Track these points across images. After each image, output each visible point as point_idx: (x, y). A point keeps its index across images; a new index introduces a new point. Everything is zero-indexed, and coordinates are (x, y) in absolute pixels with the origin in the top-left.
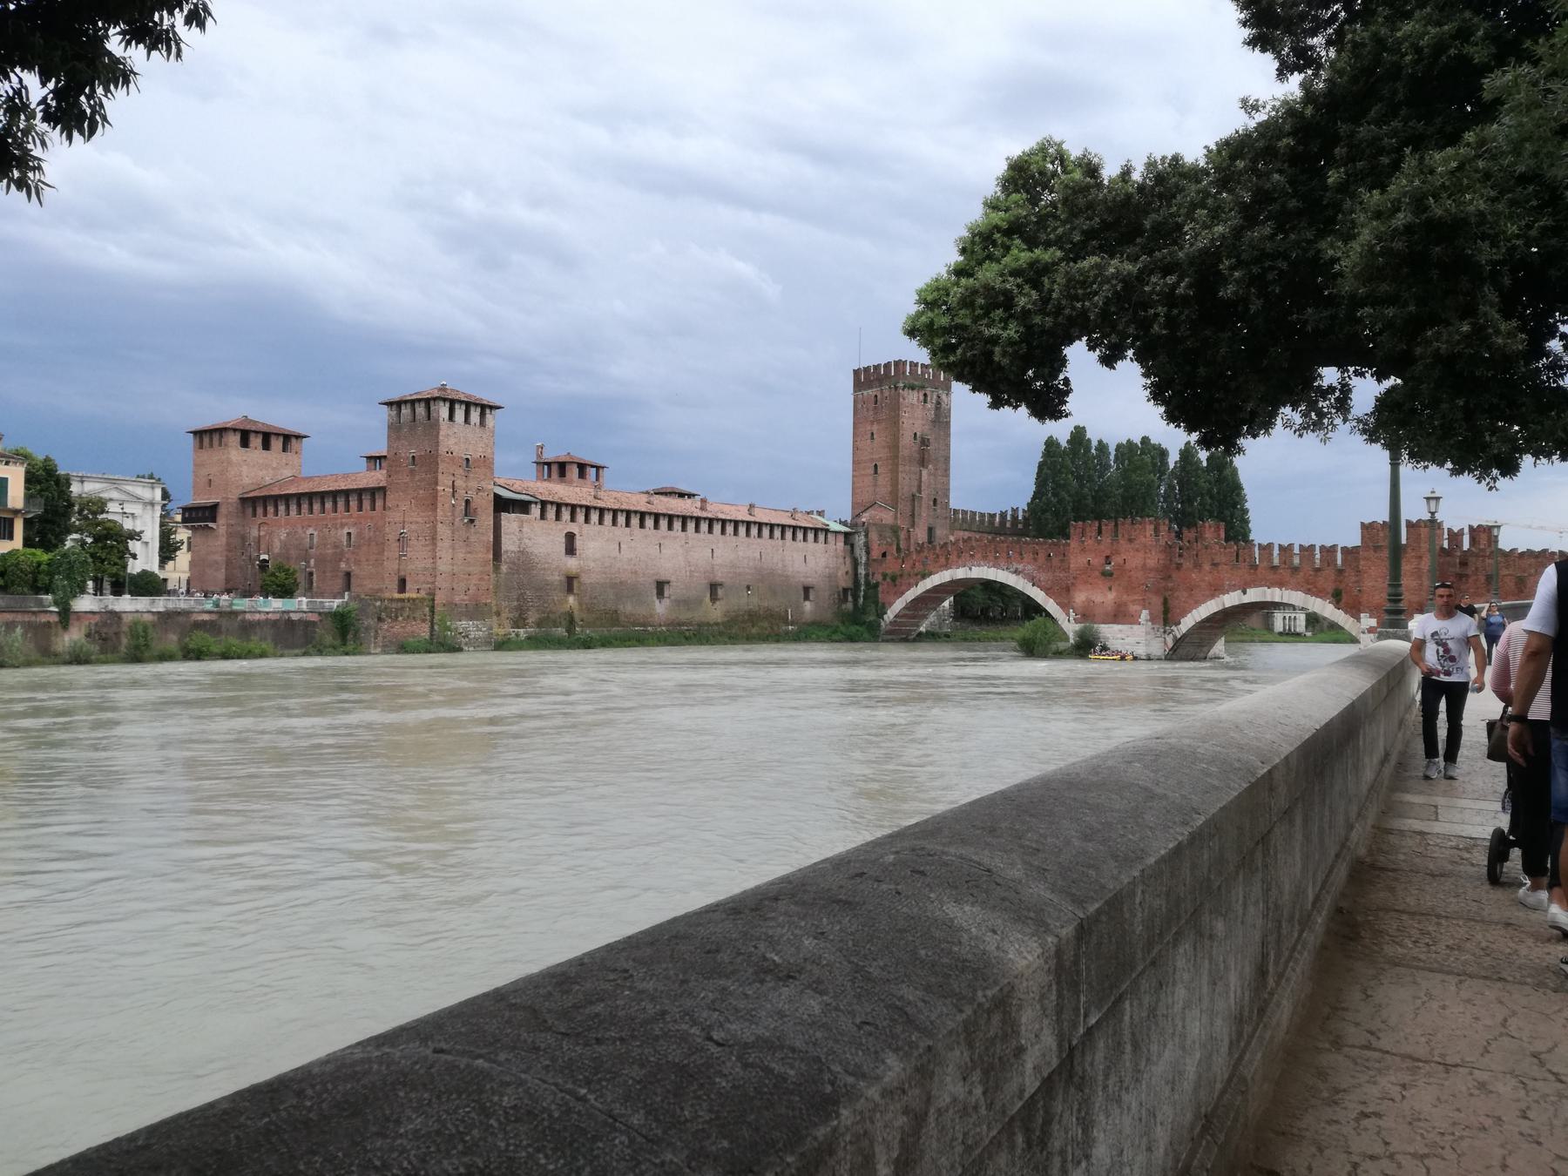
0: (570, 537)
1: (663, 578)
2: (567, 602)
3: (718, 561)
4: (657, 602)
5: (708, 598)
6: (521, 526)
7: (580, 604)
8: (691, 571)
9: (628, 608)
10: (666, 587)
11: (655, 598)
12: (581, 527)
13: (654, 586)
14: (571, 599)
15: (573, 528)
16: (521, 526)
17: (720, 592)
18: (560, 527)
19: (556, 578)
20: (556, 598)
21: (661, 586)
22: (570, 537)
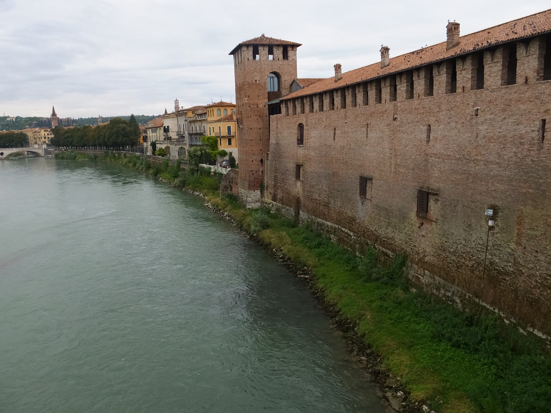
0: (301, 126)
1: (366, 174)
2: (296, 186)
3: (437, 147)
4: (360, 203)
5: (413, 215)
6: (277, 124)
7: (304, 191)
8: (397, 165)
9: (336, 204)
10: (369, 184)
11: (358, 198)
12: (307, 117)
13: (358, 181)
14: (299, 184)
15: (302, 119)
16: (277, 124)
17: (434, 208)
18: (295, 119)
19: (291, 166)
20: (291, 182)
21: (364, 181)
22: (301, 126)
